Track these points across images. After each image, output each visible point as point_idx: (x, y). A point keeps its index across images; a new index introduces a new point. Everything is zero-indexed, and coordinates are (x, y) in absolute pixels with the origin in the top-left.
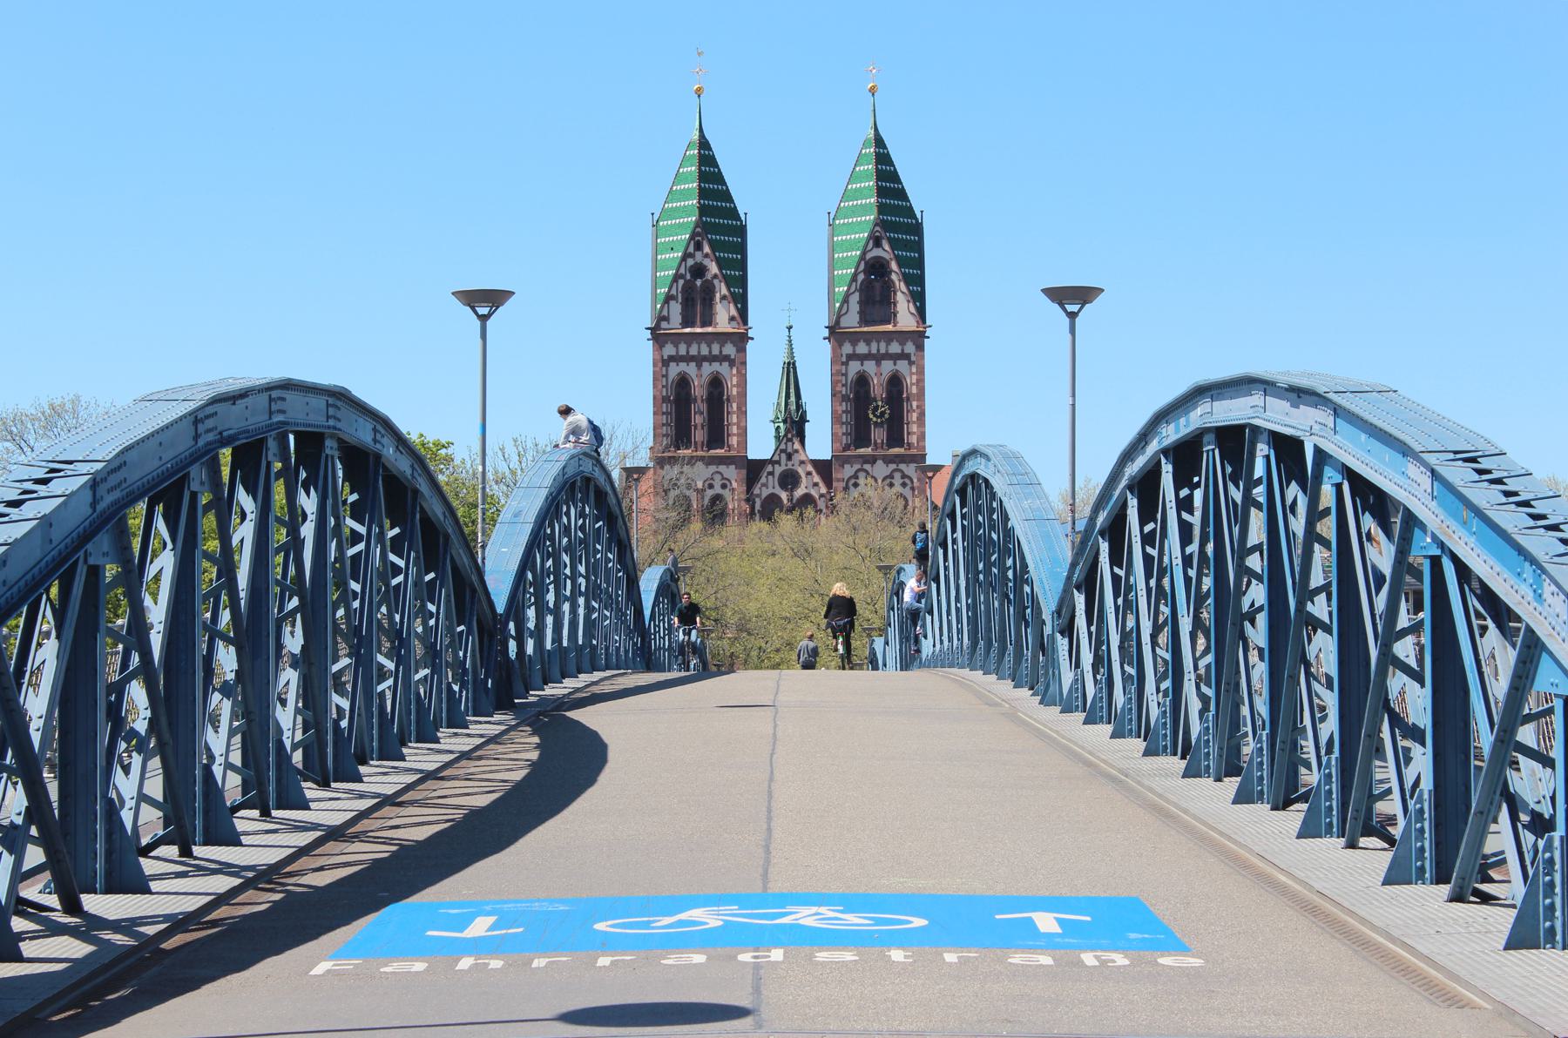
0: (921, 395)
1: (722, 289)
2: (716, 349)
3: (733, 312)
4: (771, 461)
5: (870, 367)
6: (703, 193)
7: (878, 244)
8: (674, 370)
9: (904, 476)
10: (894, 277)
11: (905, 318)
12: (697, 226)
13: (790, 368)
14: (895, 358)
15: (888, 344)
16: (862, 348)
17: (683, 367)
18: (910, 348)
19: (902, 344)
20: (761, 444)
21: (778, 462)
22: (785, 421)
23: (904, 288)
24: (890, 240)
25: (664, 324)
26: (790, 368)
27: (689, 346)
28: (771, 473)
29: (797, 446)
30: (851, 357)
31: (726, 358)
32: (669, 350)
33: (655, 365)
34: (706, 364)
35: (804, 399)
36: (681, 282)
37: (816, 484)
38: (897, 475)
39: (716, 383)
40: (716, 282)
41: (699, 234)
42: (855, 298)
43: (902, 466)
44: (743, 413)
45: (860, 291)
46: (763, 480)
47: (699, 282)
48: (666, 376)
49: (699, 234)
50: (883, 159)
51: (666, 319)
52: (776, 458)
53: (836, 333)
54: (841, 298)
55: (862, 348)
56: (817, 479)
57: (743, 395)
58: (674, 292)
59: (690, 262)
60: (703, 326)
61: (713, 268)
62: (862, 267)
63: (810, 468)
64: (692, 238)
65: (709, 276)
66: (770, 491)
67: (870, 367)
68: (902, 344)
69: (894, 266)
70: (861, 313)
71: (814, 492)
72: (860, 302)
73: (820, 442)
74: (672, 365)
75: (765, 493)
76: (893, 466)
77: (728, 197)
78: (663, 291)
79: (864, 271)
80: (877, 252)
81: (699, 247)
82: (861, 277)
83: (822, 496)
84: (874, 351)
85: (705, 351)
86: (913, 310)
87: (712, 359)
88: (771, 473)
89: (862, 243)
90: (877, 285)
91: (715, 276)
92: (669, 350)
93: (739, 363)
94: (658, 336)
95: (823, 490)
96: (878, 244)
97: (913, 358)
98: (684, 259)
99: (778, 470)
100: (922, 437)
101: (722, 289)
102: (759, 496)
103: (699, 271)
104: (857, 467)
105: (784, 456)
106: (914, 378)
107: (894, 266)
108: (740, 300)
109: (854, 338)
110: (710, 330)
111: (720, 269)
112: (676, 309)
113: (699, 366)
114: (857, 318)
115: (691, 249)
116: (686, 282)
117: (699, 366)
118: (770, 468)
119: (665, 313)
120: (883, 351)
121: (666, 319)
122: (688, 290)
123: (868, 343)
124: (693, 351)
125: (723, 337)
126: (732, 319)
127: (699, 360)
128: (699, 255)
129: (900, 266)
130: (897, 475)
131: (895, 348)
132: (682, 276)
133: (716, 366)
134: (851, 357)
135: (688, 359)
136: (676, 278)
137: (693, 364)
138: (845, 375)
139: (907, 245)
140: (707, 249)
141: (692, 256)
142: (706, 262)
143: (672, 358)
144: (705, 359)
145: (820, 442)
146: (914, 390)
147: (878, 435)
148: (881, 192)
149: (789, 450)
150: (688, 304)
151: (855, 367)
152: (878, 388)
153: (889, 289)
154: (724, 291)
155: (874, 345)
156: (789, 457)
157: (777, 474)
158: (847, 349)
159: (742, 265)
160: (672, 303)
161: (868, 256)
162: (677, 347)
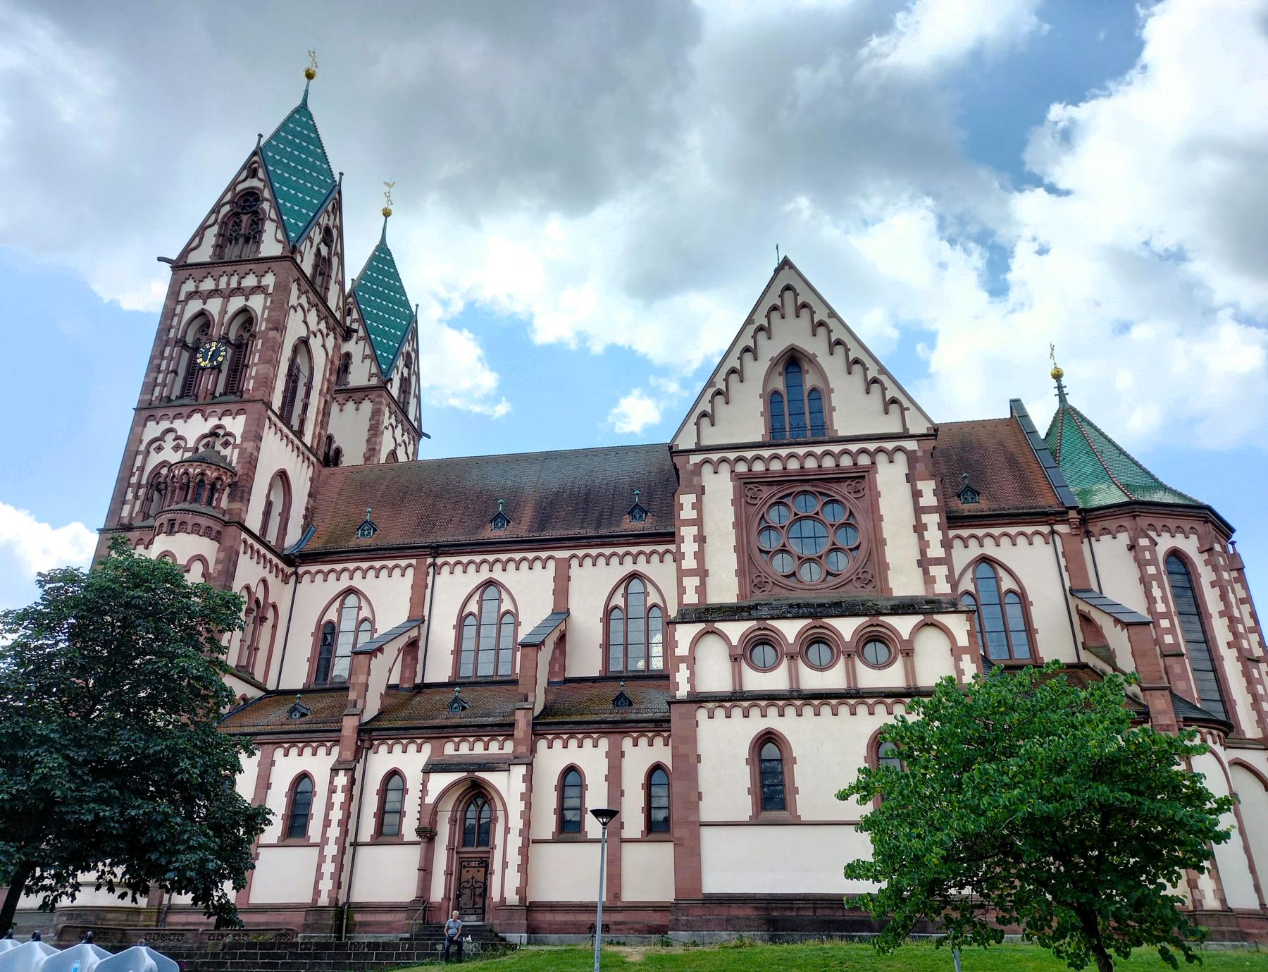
5: (214, 306)
10: (266, 205)
16: (209, 284)
23: (273, 216)
43: (227, 421)
45: (224, 223)
55: (209, 284)
67: (214, 306)
69: (267, 194)
70: (219, 247)
72: (220, 235)
80: (254, 183)
82: (226, 208)
84: (223, 285)
86: (280, 236)
96: (253, 173)
97: (270, 291)
104: (165, 424)
107: (267, 194)
114: (211, 251)
120: (234, 284)
131: (250, 281)
151: (194, 306)
155: (223, 281)
158: (189, 286)
161: (240, 187)
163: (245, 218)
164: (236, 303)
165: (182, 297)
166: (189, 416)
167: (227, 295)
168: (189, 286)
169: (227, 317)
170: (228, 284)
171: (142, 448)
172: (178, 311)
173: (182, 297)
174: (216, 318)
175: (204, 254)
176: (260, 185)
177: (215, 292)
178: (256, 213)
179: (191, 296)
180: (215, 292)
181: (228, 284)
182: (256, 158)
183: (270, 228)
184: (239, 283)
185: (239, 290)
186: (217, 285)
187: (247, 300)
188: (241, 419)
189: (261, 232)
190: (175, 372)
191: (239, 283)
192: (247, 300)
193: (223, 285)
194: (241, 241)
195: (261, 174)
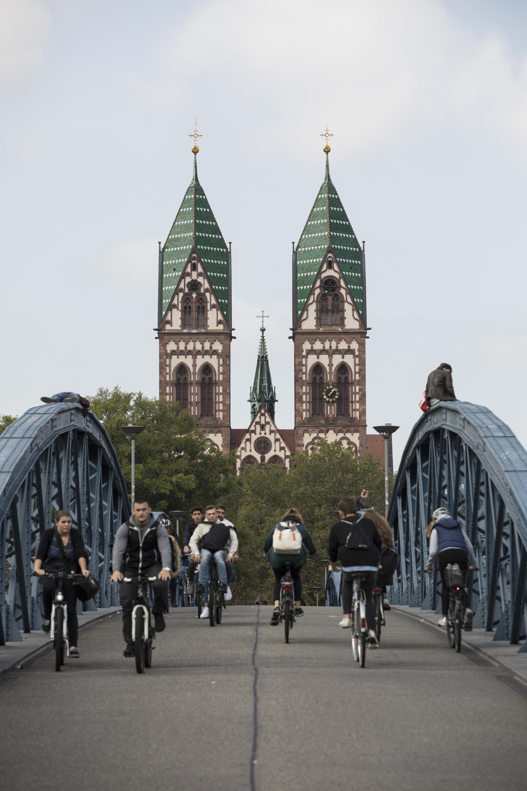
0: (362, 381)
1: (211, 299)
2: (207, 346)
3: (220, 317)
4: (247, 431)
6: (198, 228)
7: (330, 266)
8: (175, 361)
10: (343, 291)
11: (351, 323)
12: (194, 251)
13: (263, 362)
14: (344, 353)
16: (318, 346)
17: (182, 359)
18: (354, 345)
19: (349, 343)
20: (241, 417)
21: (254, 432)
22: (259, 401)
23: (349, 300)
24: (338, 263)
25: (168, 327)
26: (263, 362)
27: (187, 344)
28: (249, 440)
29: (268, 419)
30: (311, 351)
31: (215, 352)
32: (171, 346)
33: (161, 357)
34: (199, 357)
35: (274, 384)
36: (181, 295)
39: (207, 369)
40: (208, 295)
41: (194, 258)
42: (312, 308)
43: (348, 435)
44: (227, 393)
45: (317, 302)
46: (243, 445)
47: (194, 295)
48: (170, 366)
49: (194, 258)
50: (334, 202)
51: (170, 323)
52: (252, 428)
53: (298, 334)
54: (302, 307)
55: (318, 346)
56: (283, 445)
57: (227, 381)
58: (175, 302)
59: (188, 279)
60: (197, 327)
61: (207, 285)
62: (318, 284)
63: (278, 436)
64: (189, 261)
65: (202, 291)
66: (248, 453)
67: (324, 360)
68: (349, 343)
69: (342, 283)
70: (318, 318)
71: (281, 454)
73: (285, 417)
74: (174, 357)
75: (244, 455)
76: (341, 435)
77: (216, 230)
78: (166, 301)
79: (320, 287)
81: (194, 268)
82: (317, 291)
83: (286, 457)
84: (327, 347)
85: (199, 347)
87: (204, 353)
88: (248, 440)
89: (318, 267)
90: (330, 298)
91: (207, 290)
92: (171, 346)
93: (225, 356)
94: (163, 335)
95: (288, 453)
96: (330, 266)
97: (357, 353)
98: (183, 277)
99: (254, 437)
100: (363, 413)
101: (211, 299)
102: (239, 457)
103: (194, 286)
104: (314, 435)
105: (258, 427)
106: (357, 367)
107: (342, 283)
108: (225, 309)
109: (311, 335)
110: (203, 331)
111: (211, 284)
112: (176, 316)
113: (194, 358)
115: (189, 270)
116: (185, 294)
117: (194, 358)
118: (247, 436)
119: (169, 318)
120: (334, 347)
121: (170, 323)
122: (187, 298)
123: (323, 342)
124: (190, 347)
125: (214, 335)
126: (219, 322)
127: (195, 354)
128: (194, 275)
129: (346, 283)
131: (343, 345)
132: (182, 290)
133: (207, 359)
134: (311, 351)
135: (186, 353)
136: (177, 291)
137: (190, 357)
138: (306, 365)
139: (352, 268)
140: (200, 269)
141: (189, 275)
142: (201, 280)
143: (173, 352)
144: (199, 353)
145: (285, 417)
146: (357, 378)
147: (331, 411)
148: (333, 227)
149: (263, 422)
150: (186, 311)
151: (312, 360)
152: (330, 377)
153: (338, 299)
154: (214, 302)
156: (263, 427)
157: (253, 441)
158: (307, 346)
159: (227, 282)
160: (174, 310)
161: (323, 276)
162: (177, 344)
163: (330, 298)
164: (337, 360)
165: (304, 353)
166: (327, 432)
167: (331, 353)
168: (307, 346)
169: (334, 368)
170: (330, 347)
171: (304, 449)
172: (304, 363)
173: (304, 353)
174: (328, 368)
175: (310, 323)
176: (337, 276)
177: (323, 351)
178: (336, 295)
180: (323, 351)
181: (330, 347)
182: (330, 255)
183: (348, 308)
184: (337, 347)
185: (337, 351)
186: (324, 347)
187: (343, 358)
188: (357, 435)
189: (343, 311)
191: (337, 347)
192: (343, 358)
193: (327, 347)
194: (330, 313)
195: (335, 266)
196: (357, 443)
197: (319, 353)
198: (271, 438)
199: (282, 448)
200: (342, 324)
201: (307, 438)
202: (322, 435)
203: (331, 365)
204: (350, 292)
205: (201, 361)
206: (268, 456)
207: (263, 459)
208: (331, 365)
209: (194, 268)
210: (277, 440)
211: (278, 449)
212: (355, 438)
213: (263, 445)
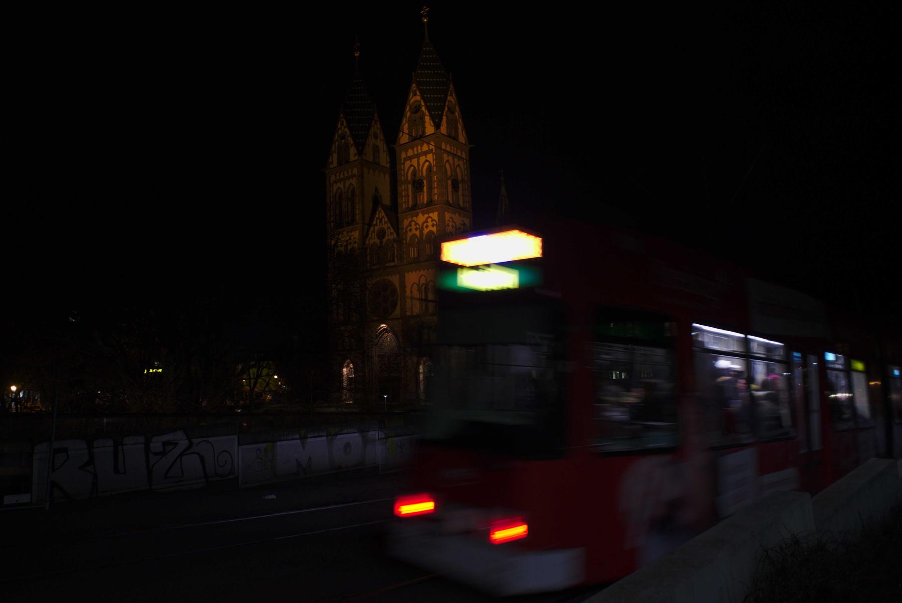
5: (415, 162)
9: (433, 220)
15: (422, 146)
16: (410, 153)
17: (339, 185)
19: (428, 144)
21: (376, 225)
31: (353, 176)
32: (333, 178)
37: (391, 233)
38: (430, 220)
43: (431, 215)
51: (332, 163)
55: (410, 153)
56: (392, 231)
76: (426, 216)
81: (342, 124)
82: (408, 114)
99: (377, 228)
104: (410, 219)
107: (423, 103)
118: (372, 229)
124: (342, 176)
126: (355, 155)
130: (430, 220)
156: (381, 222)
167: (418, 156)
168: (403, 155)
179: (405, 159)
183: (427, 119)
188: (436, 213)
190: (408, 196)
196: (436, 218)
197: (410, 158)
198: (385, 226)
199: (391, 233)
200: (424, 132)
201: (406, 223)
202: (414, 218)
203: (419, 165)
204: (427, 108)
205: (348, 184)
206: (385, 240)
207: (381, 242)
208: (419, 165)
209: (342, 124)
210: (389, 228)
211: (391, 235)
212: (435, 215)
213: (381, 234)
